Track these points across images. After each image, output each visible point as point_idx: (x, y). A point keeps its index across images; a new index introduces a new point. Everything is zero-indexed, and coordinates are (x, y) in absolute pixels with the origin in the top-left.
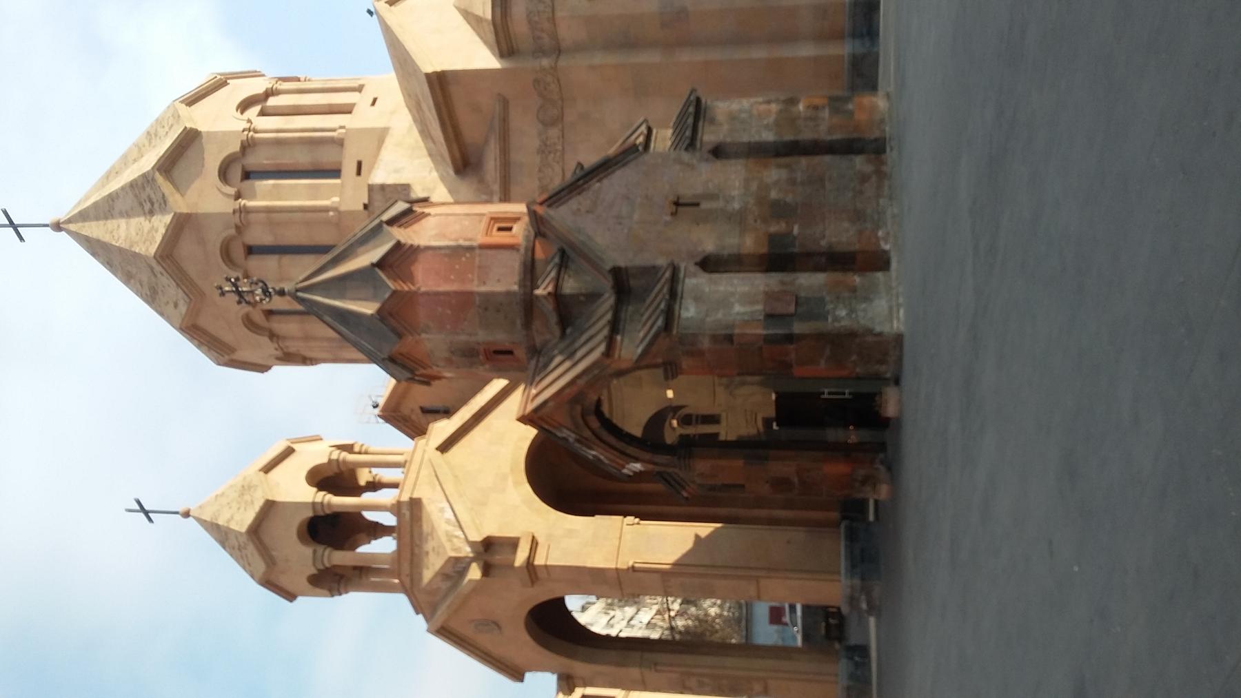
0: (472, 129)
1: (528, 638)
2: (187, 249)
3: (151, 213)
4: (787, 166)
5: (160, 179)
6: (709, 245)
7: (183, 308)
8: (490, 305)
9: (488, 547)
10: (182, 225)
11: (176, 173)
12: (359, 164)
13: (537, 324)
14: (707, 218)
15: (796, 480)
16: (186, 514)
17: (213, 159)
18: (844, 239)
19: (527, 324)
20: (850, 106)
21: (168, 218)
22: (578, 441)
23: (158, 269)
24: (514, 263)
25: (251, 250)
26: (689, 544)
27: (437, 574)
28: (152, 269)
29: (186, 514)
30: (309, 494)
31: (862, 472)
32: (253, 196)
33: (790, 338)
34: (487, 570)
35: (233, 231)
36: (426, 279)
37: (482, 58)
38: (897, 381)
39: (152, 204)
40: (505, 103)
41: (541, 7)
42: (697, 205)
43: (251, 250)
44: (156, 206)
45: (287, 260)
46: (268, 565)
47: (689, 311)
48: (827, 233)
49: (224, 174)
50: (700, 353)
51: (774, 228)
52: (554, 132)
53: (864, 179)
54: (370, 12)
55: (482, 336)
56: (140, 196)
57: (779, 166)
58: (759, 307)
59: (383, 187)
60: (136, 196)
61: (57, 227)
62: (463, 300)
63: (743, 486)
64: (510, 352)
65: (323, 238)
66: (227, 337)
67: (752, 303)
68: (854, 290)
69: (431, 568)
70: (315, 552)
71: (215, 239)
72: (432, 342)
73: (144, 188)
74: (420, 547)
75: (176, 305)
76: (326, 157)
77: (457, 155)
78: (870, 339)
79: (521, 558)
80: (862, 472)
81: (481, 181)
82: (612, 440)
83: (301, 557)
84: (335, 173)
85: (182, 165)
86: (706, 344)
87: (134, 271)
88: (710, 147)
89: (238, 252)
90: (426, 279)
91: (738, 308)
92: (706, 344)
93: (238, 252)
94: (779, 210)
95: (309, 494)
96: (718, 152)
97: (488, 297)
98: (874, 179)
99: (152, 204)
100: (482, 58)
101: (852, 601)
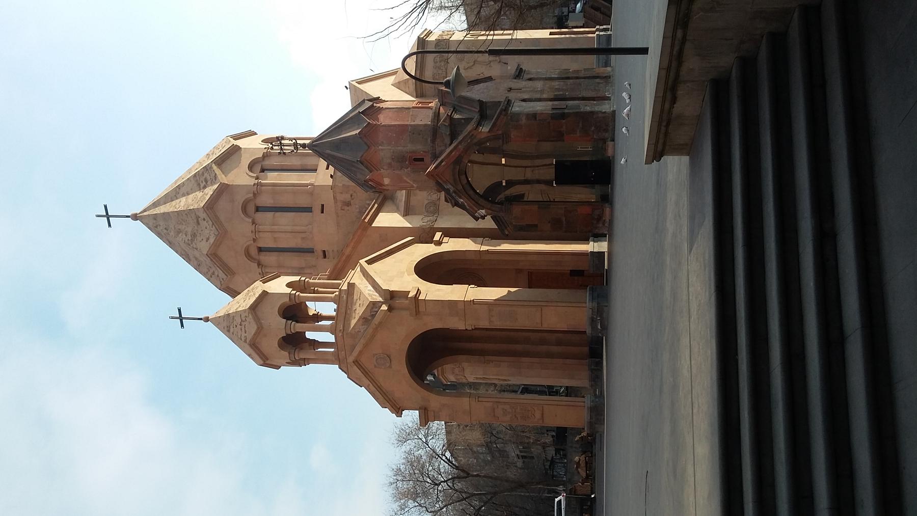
1: (405, 371)
3: (205, 187)
5: (215, 167)
7: (212, 240)
8: (415, 131)
9: (391, 296)
14: (524, 92)
15: (564, 219)
16: (207, 319)
17: (246, 161)
19: (433, 141)
22: (455, 192)
23: (202, 215)
24: (430, 113)
25: (258, 209)
26: (505, 293)
27: (360, 317)
28: (198, 218)
29: (207, 319)
30: (288, 290)
31: (597, 212)
32: (266, 179)
33: (563, 116)
34: (390, 309)
36: (384, 119)
38: (613, 140)
39: (206, 182)
41: (440, 72)
45: (278, 214)
46: (258, 328)
49: (251, 167)
55: (410, 147)
56: (200, 179)
61: (135, 217)
62: (402, 129)
63: (536, 226)
64: (422, 160)
65: (303, 202)
66: (232, 263)
69: (359, 310)
71: (240, 199)
72: (384, 152)
73: (203, 174)
74: (351, 309)
75: (208, 239)
78: (600, 115)
79: (411, 295)
80: (597, 212)
82: (471, 193)
83: (278, 326)
85: (228, 162)
86: (524, 121)
87: (182, 227)
89: (251, 208)
90: (384, 119)
92: (524, 121)
93: (251, 208)
94: (558, 90)
95: (288, 290)
97: (415, 127)
99: (206, 182)
101: (593, 321)
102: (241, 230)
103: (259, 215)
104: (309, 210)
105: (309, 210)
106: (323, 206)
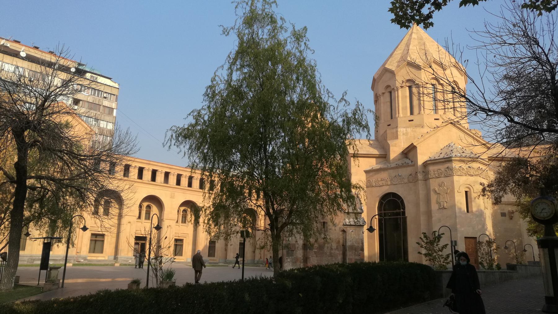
0: (410, 155)
2: (388, 75)
4: (337, 248)
10: (392, 73)
12: (412, 120)
21: (393, 69)
35: (392, 88)
37: (421, 159)
43: (391, 92)
45: (389, 104)
49: (408, 81)
52: (406, 181)
57: (337, 246)
59: (397, 131)
68: (295, 262)
76: (416, 110)
77: (406, 152)
81: (399, 160)
84: (412, 113)
88: (345, 229)
89: (389, 90)
93: (389, 90)
96: (344, 231)
100: (421, 159)
102: (381, 89)
103: (387, 95)
104: (392, 118)
105: (392, 118)
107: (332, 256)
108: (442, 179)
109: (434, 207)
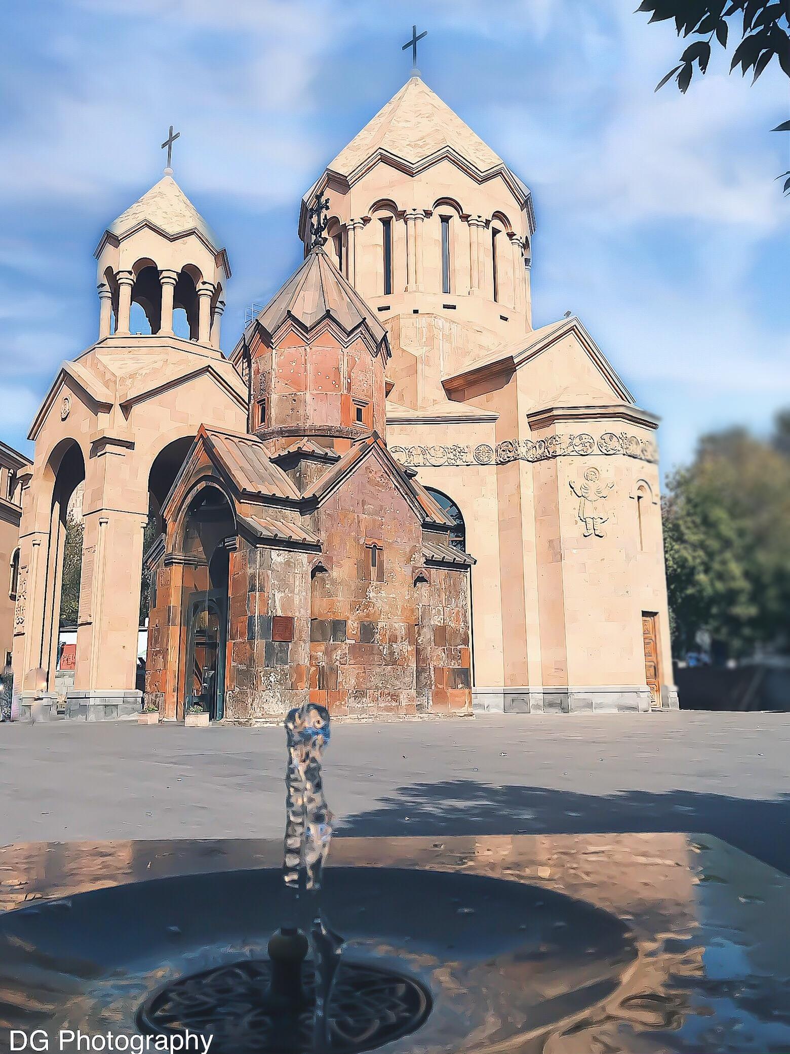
6: (335, 573)
11: (446, 164)
12: (454, 307)
13: (283, 440)
18: (340, 680)
19: (281, 433)
20: (460, 686)
25: (386, 222)
33: (252, 638)
39: (421, 147)
40: (494, 419)
42: (374, 565)
44: (420, 150)
45: (380, 252)
47: (278, 557)
48: (346, 667)
50: (243, 567)
51: (353, 626)
52: (470, 458)
53: (395, 697)
54: (568, 314)
58: (279, 613)
60: (428, 135)
67: (283, 609)
70: (130, 273)
77: (455, 384)
88: (425, 574)
89: (385, 213)
91: (278, 596)
93: (385, 213)
94: (368, 631)
98: (394, 704)
104: (388, 290)
105: (388, 290)
106: (388, 308)
107: (394, 663)
108: (591, 461)
109: (570, 530)
